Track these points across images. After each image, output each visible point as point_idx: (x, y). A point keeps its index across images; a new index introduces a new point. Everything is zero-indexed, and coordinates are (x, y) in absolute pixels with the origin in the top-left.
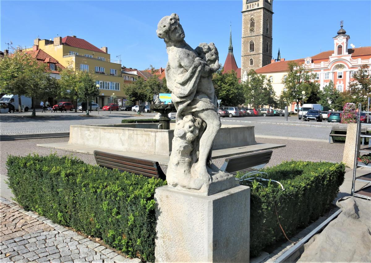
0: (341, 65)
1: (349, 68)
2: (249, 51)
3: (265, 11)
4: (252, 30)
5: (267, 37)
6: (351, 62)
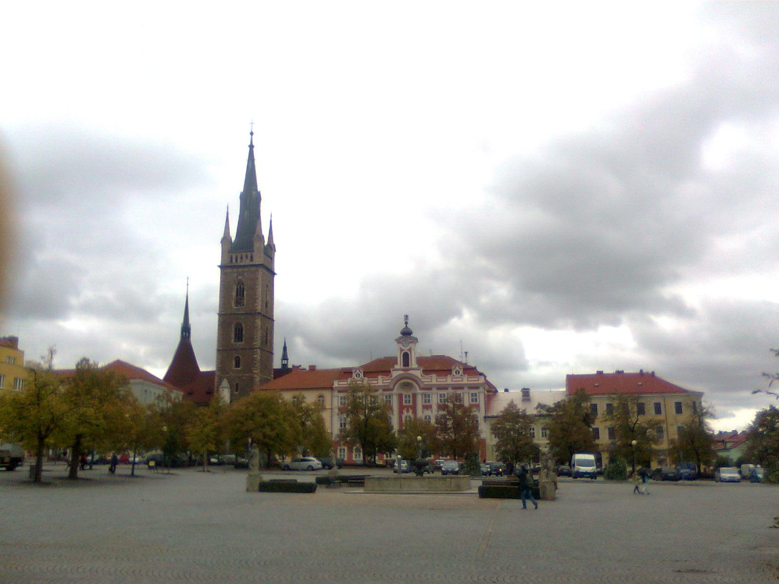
0: (408, 383)
1: (421, 389)
4: (238, 303)
6: (422, 380)
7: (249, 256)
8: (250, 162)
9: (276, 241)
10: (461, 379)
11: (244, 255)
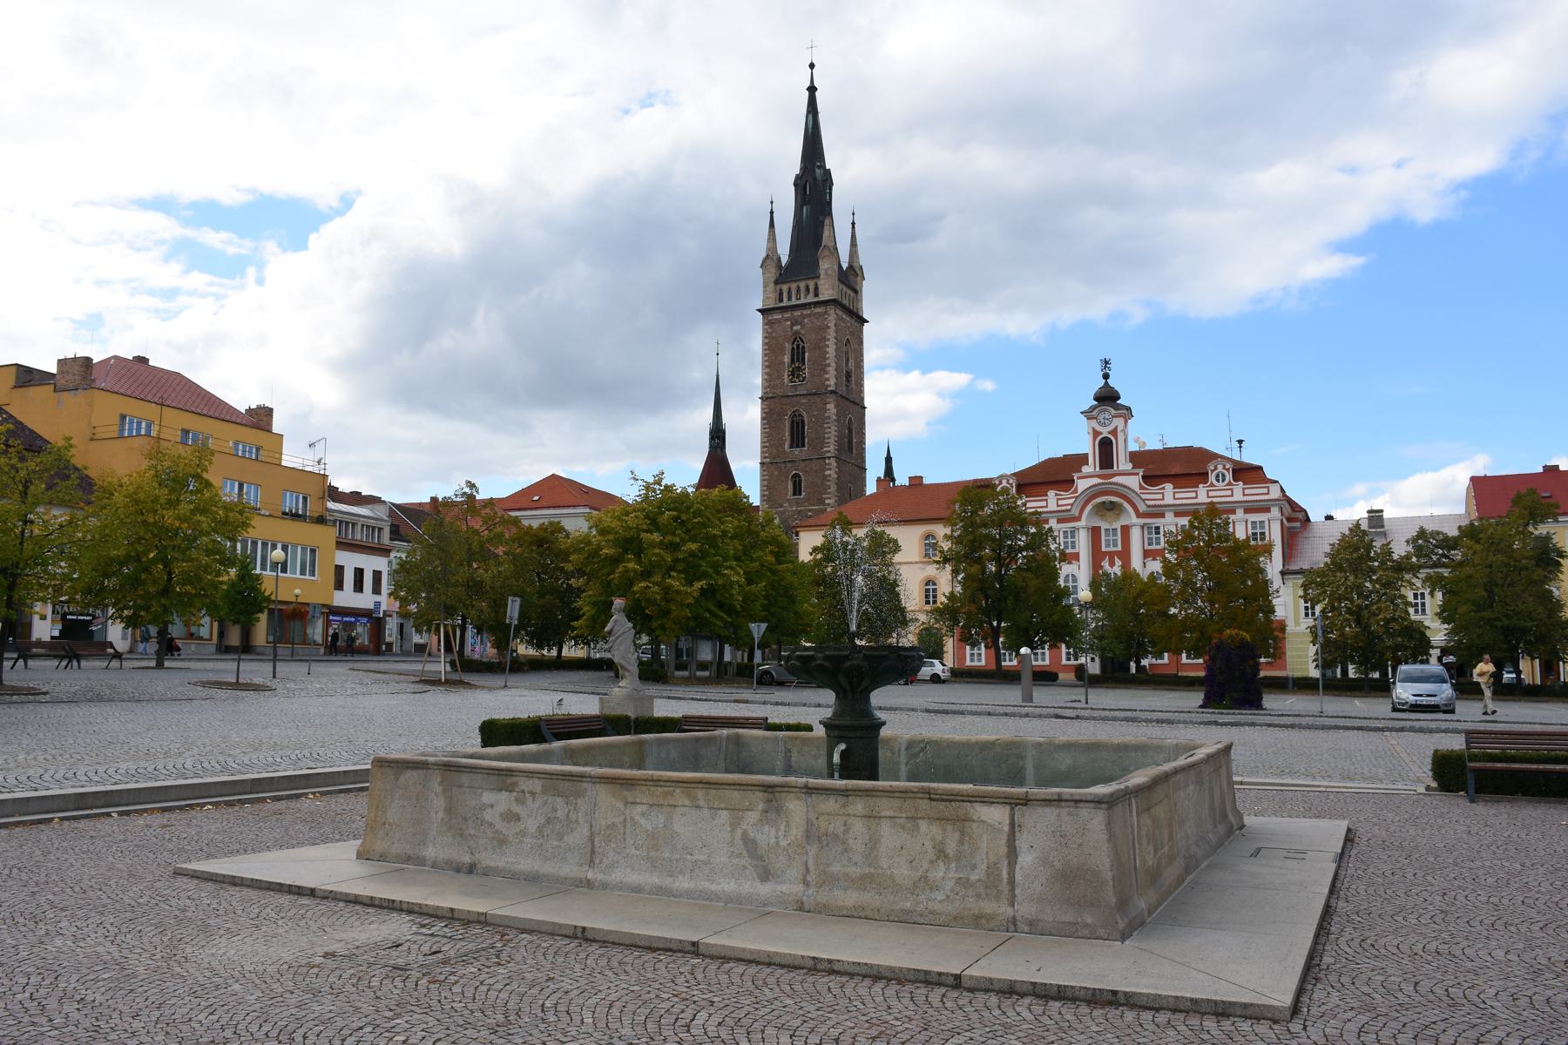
0: (1111, 502)
1: (1139, 515)
2: (787, 447)
3: (840, 313)
4: (795, 373)
5: (847, 399)
6: (1144, 496)
8: (810, 117)
9: (863, 260)
10: (1229, 493)
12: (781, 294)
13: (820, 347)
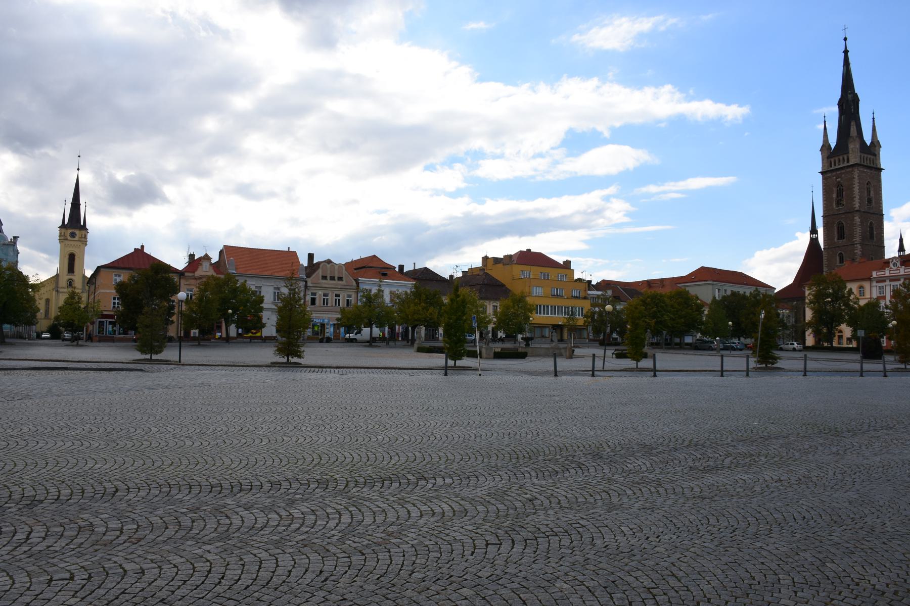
4: (839, 203)
7: (846, 158)
9: (880, 138)
11: (837, 159)
12: (831, 163)
13: (851, 189)
